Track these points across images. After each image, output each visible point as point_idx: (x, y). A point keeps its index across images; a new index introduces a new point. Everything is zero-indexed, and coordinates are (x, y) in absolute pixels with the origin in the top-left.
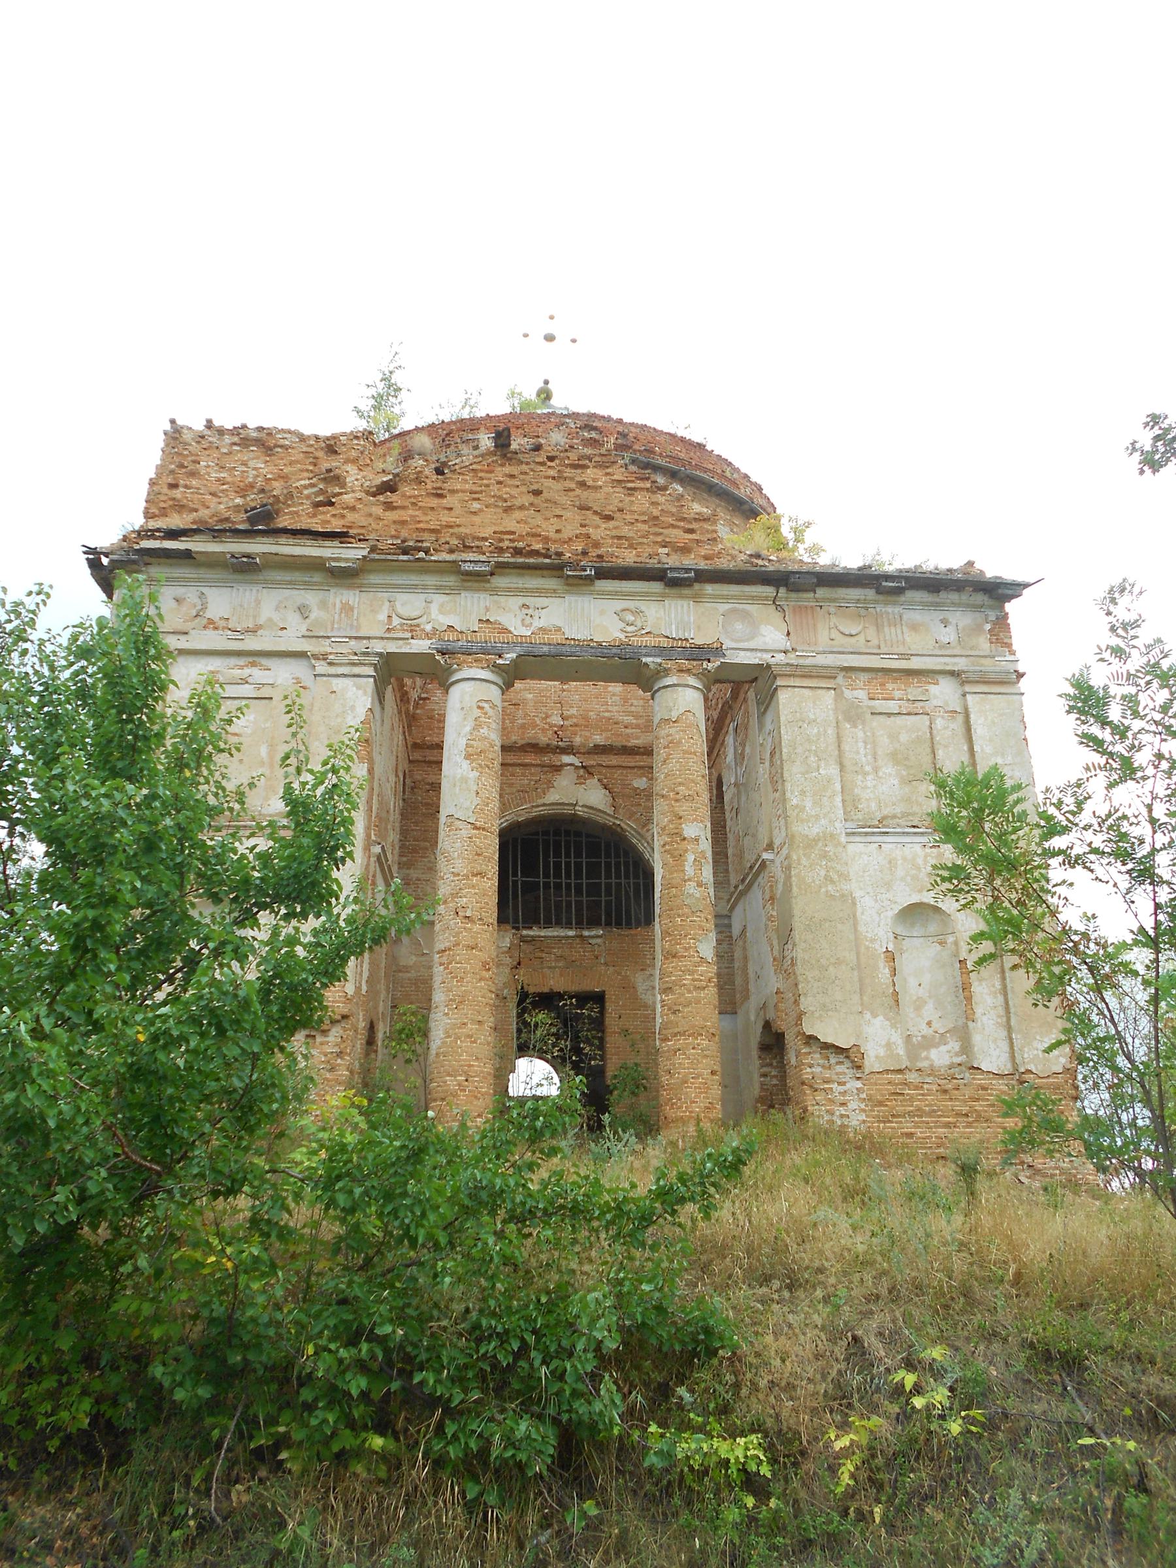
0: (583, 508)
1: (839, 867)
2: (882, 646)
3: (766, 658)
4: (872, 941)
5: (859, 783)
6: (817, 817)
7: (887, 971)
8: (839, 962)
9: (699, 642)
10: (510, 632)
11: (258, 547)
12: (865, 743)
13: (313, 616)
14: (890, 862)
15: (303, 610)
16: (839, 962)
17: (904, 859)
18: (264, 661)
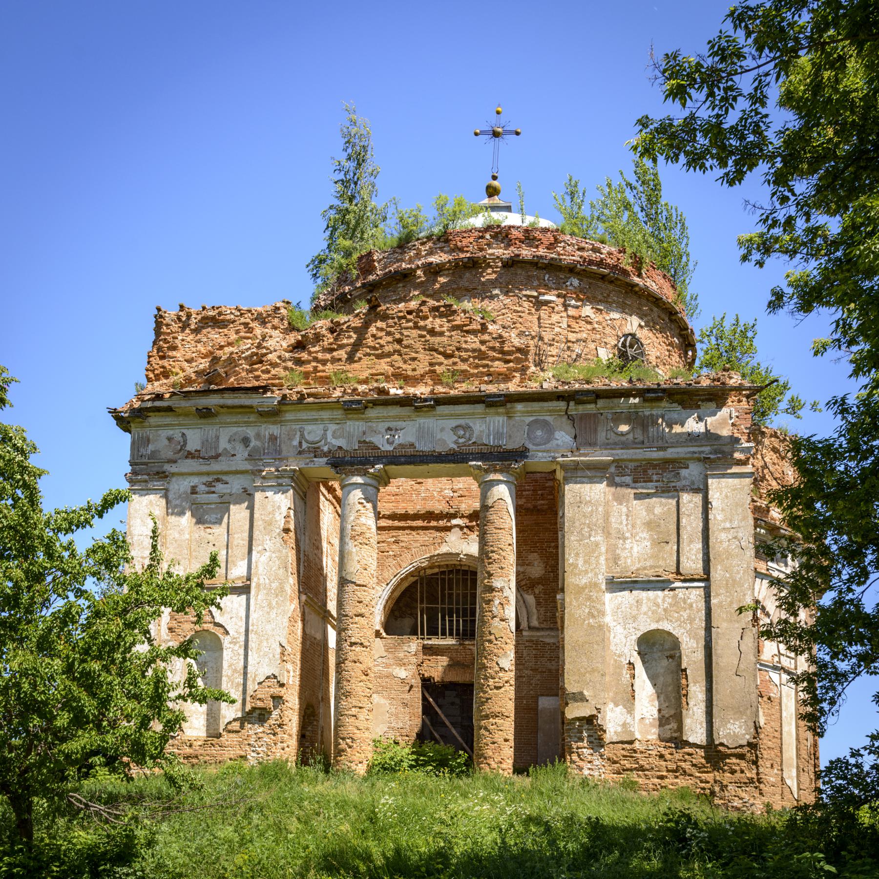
1: (598, 606)
2: (646, 441)
4: (620, 656)
5: (620, 546)
6: (586, 572)
7: (628, 676)
9: (510, 447)
10: (379, 449)
11: (213, 401)
13: (252, 445)
14: (637, 602)
15: (246, 441)
18: (224, 478)
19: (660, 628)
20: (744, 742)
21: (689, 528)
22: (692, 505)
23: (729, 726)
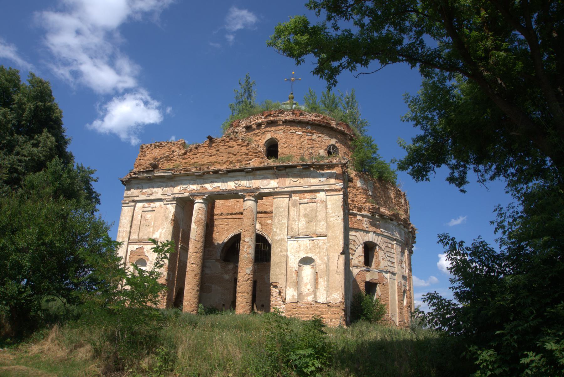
0: (229, 153)
3: (271, 190)
4: (292, 268)
6: (280, 234)
8: (281, 274)
12: (297, 212)
16: (281, 274)
17: (304, 245)
19: (308, 256)
20: (338, 302)
21: (320, 216)
22: (321, 207)
23: (333, 295)
